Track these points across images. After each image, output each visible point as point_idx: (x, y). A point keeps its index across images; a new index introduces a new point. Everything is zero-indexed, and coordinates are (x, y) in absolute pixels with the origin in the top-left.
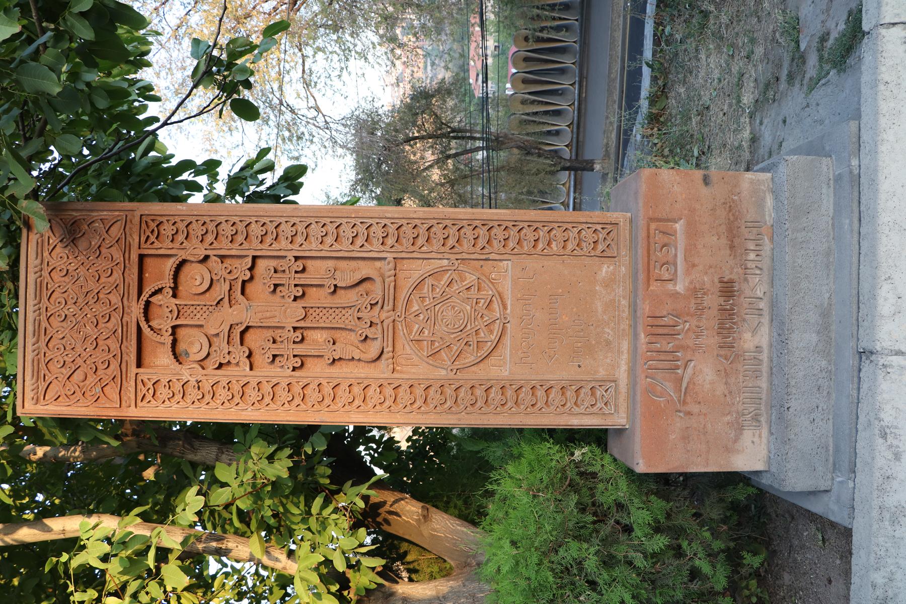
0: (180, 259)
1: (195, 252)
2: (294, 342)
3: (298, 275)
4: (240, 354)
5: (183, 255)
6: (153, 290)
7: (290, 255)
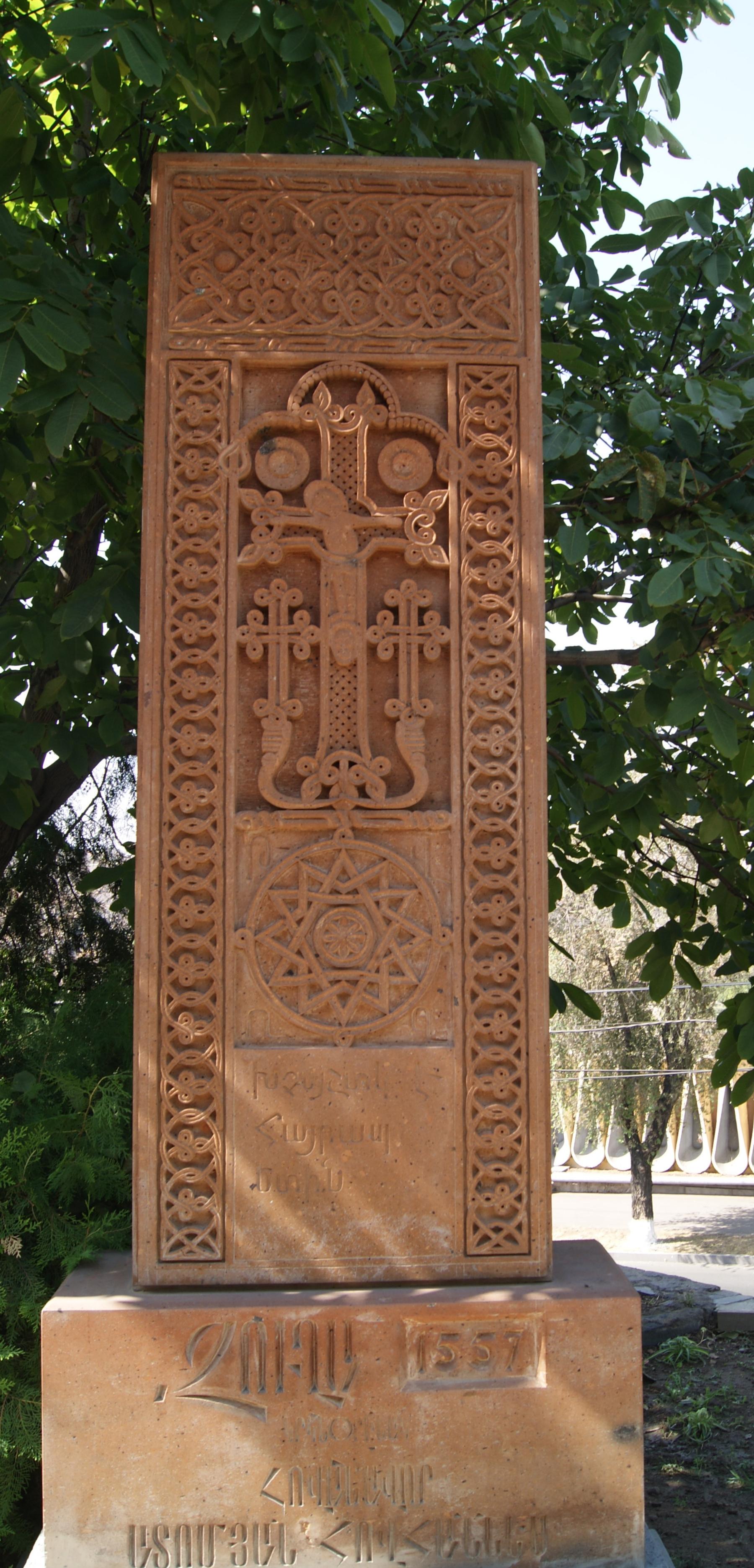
0: (439, 438)
1: (453, 463)
2: (291, 647)
3: (415, 651)
4: (266, 548)
5: (447, 444)
6: (382, 389)
7: (450, 635)
